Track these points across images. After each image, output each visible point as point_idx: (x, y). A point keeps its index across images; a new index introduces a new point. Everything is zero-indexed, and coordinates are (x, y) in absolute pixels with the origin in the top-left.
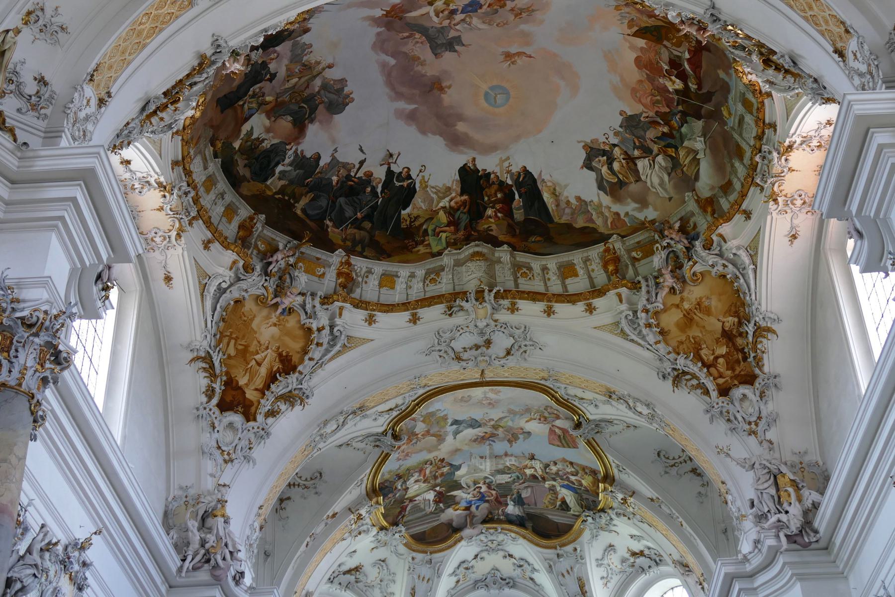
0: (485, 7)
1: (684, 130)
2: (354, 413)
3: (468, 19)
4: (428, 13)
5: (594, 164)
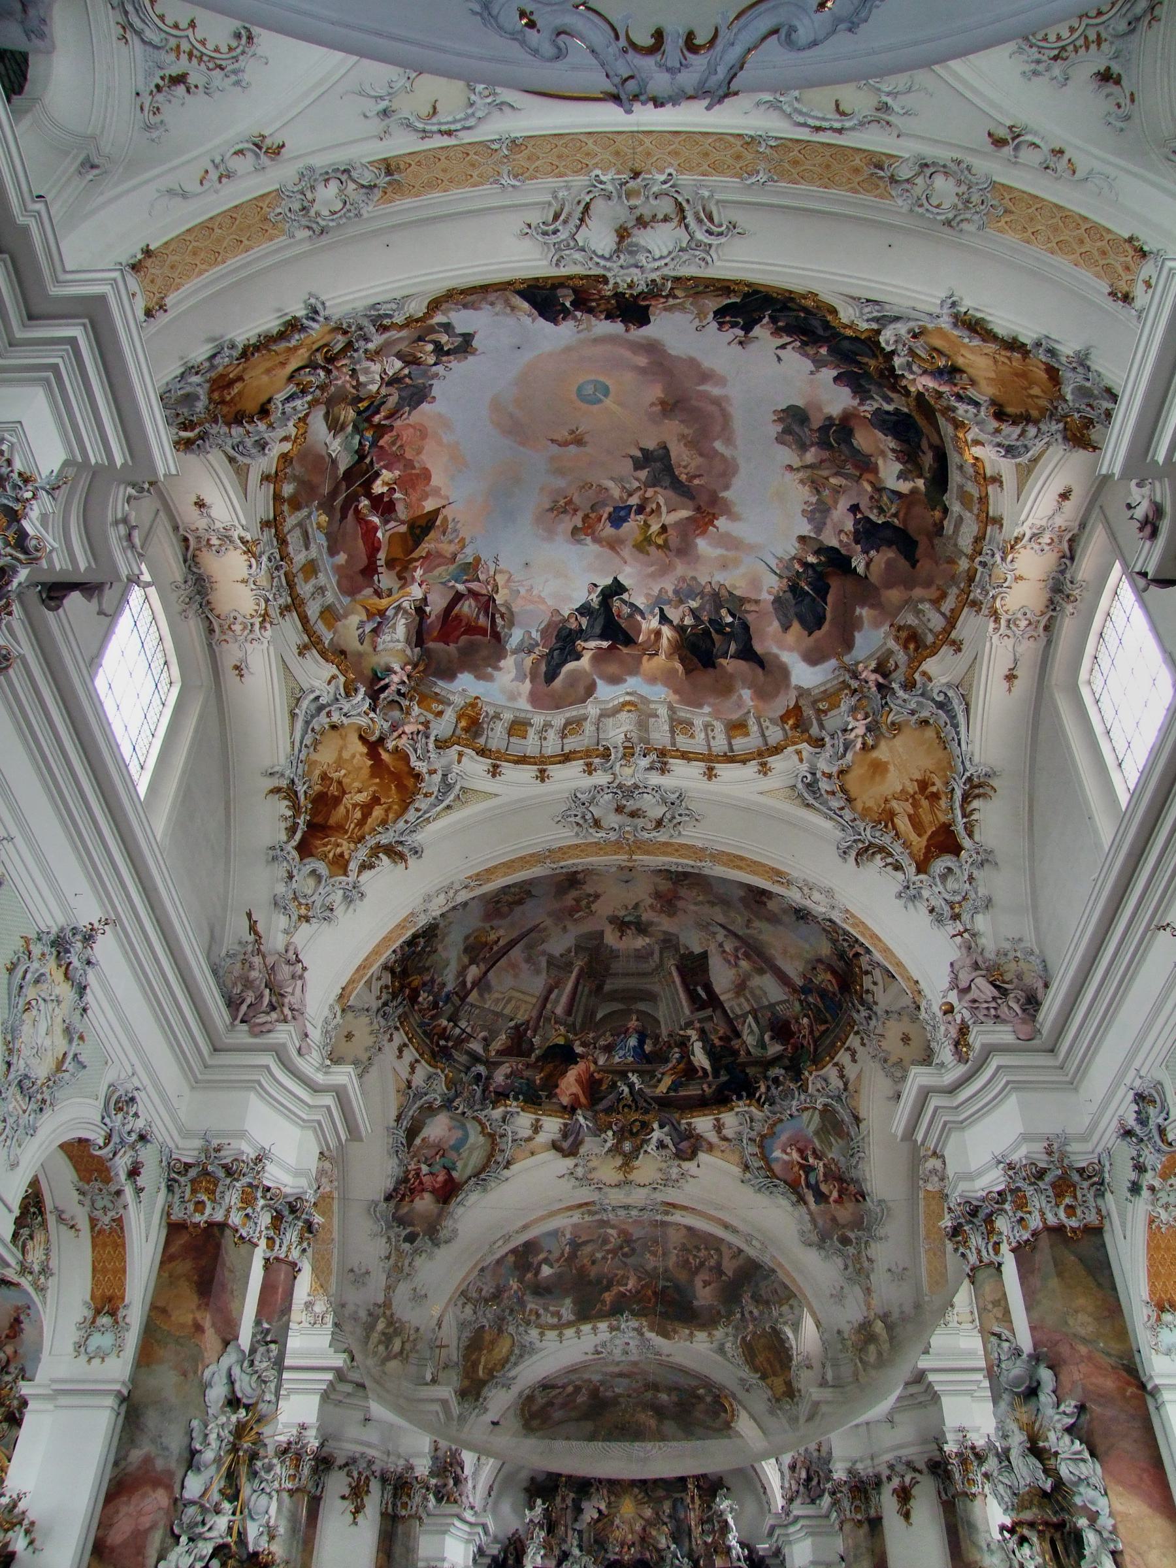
0: (605, 516)
1: (358, 437)
2: (893, 180)
3: (625, 496)
4: (669, 512)
5: (460, 339)
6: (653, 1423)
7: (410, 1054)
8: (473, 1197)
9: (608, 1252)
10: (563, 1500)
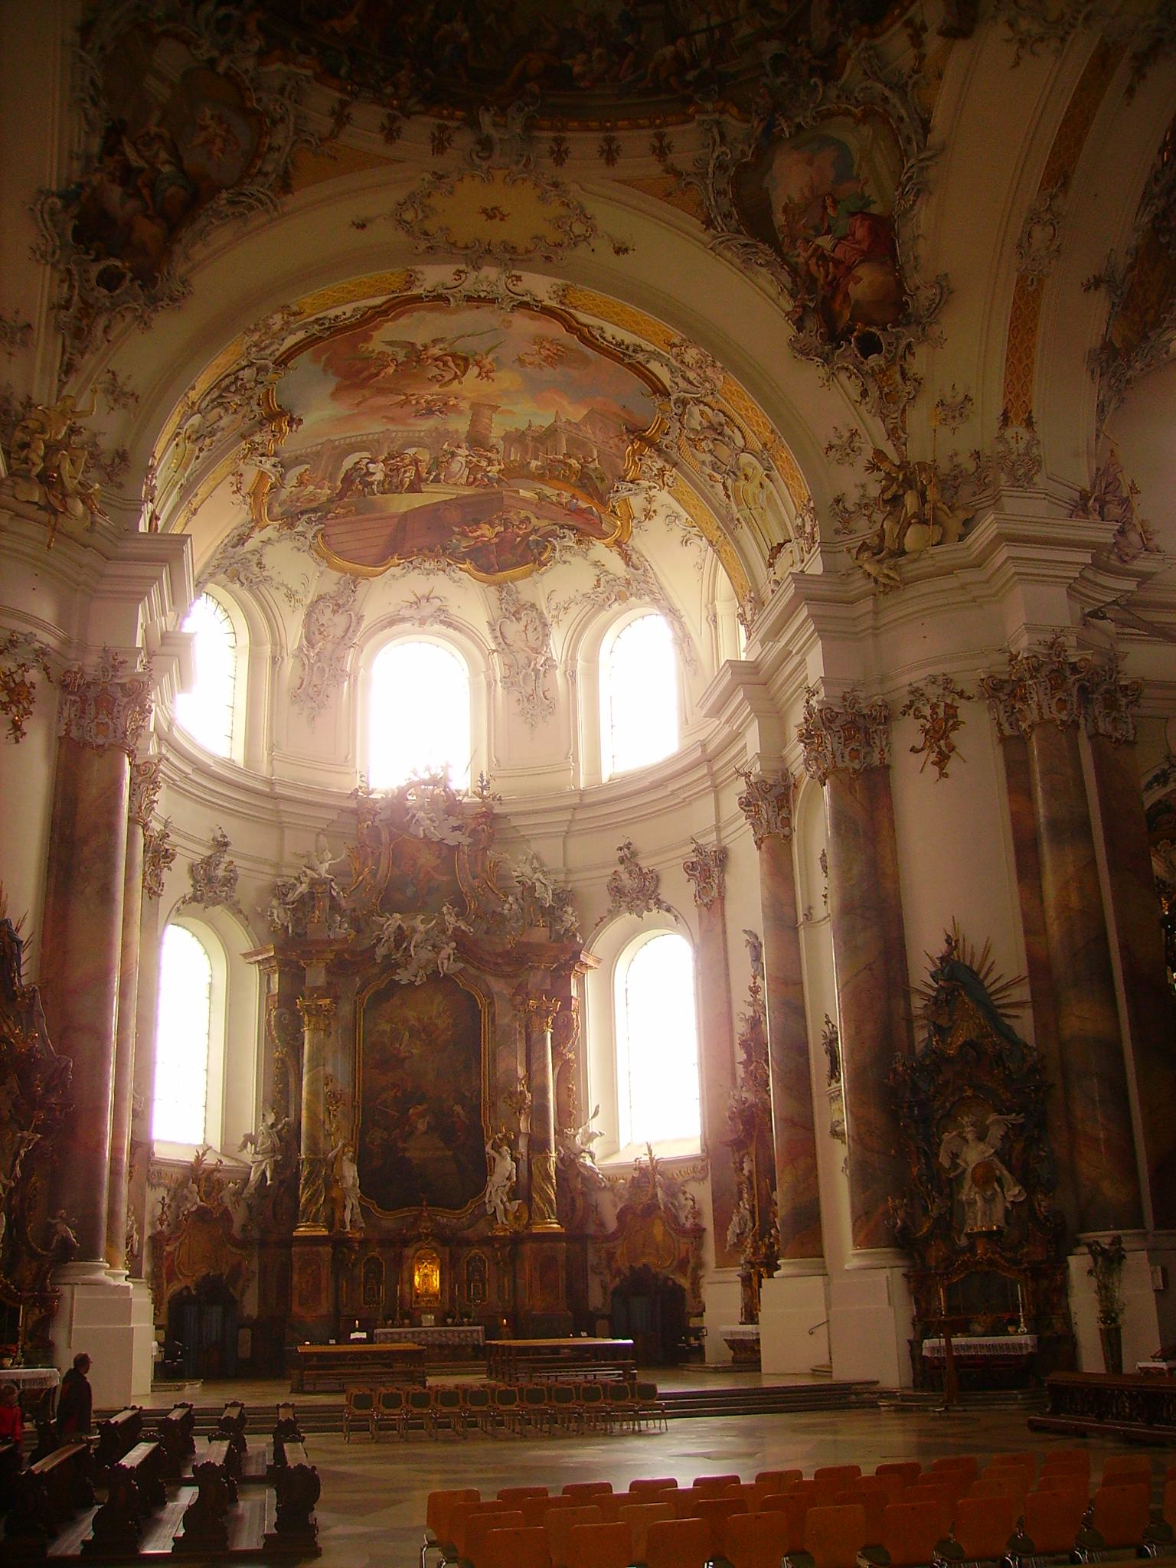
7: (636, 142)
8: (924, 216)
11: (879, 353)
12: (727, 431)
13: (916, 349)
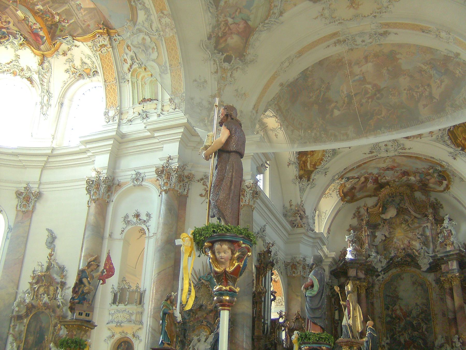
6: (408, 192)
9: (369, 98)
10: (365, 232)
11: (229, 64)
12: (150, 50)
13: (239, 70)
